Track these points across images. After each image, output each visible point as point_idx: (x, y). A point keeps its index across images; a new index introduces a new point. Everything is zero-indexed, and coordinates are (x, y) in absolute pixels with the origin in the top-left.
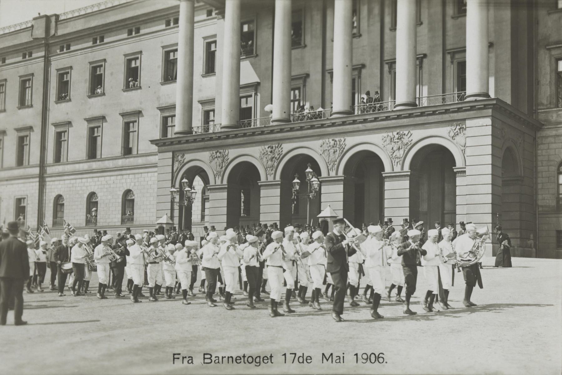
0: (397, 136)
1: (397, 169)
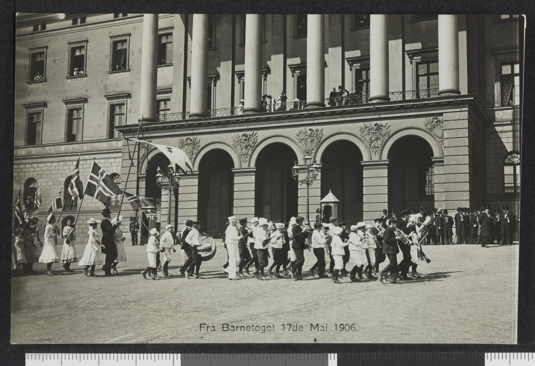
0: (376, 127)
1: (376, 158)
